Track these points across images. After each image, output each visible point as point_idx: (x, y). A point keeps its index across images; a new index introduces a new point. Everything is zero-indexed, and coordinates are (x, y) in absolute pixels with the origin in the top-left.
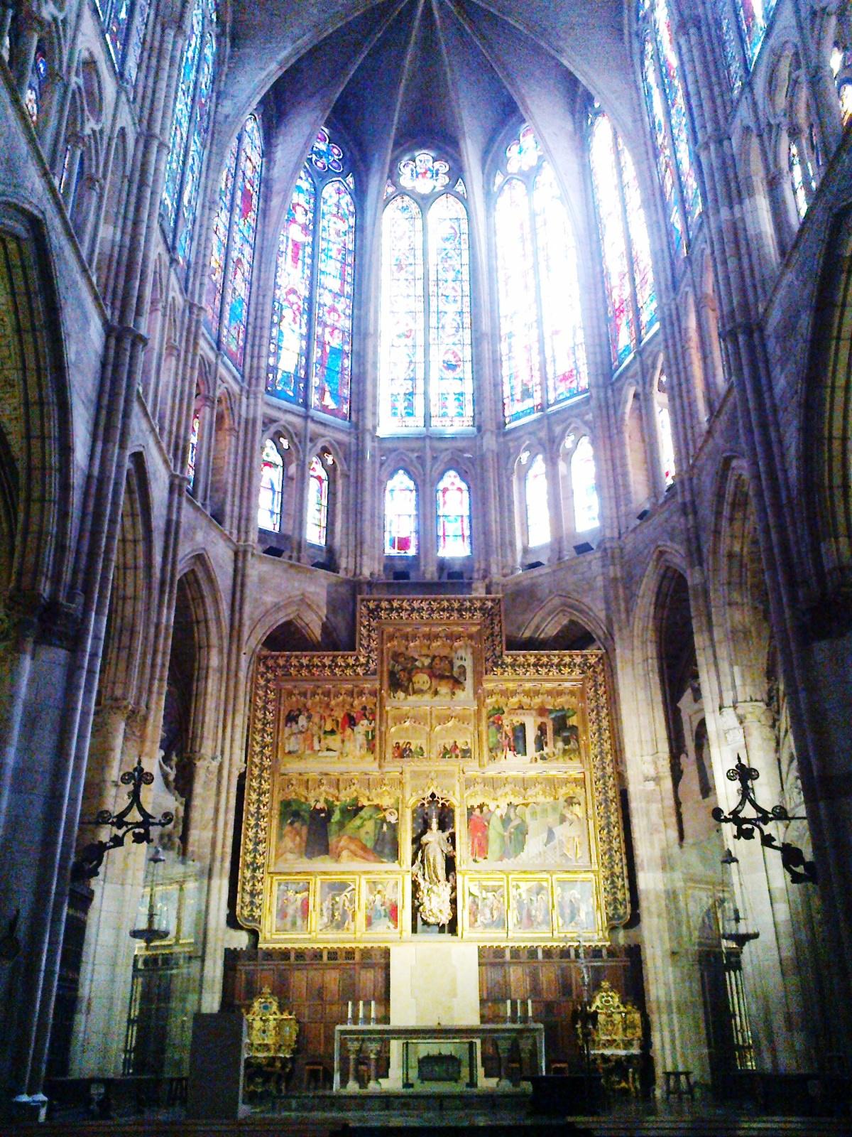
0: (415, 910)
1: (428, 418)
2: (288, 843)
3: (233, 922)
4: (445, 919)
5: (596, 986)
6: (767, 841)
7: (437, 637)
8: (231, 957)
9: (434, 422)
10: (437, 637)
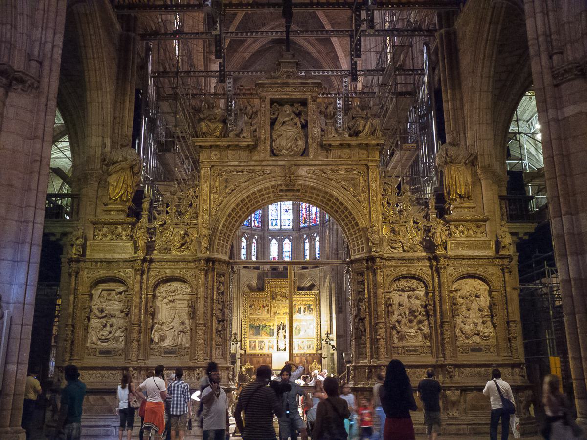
0: (277, 346)
1: (281, 226)
2: (251, 332)
3: (241, 349)
4: (283, 348)
5: (313, 361)
6: (330, 344)
7: (282, 287)
8: (241, 355)
9: (283, 227)
10: (282, 287)
